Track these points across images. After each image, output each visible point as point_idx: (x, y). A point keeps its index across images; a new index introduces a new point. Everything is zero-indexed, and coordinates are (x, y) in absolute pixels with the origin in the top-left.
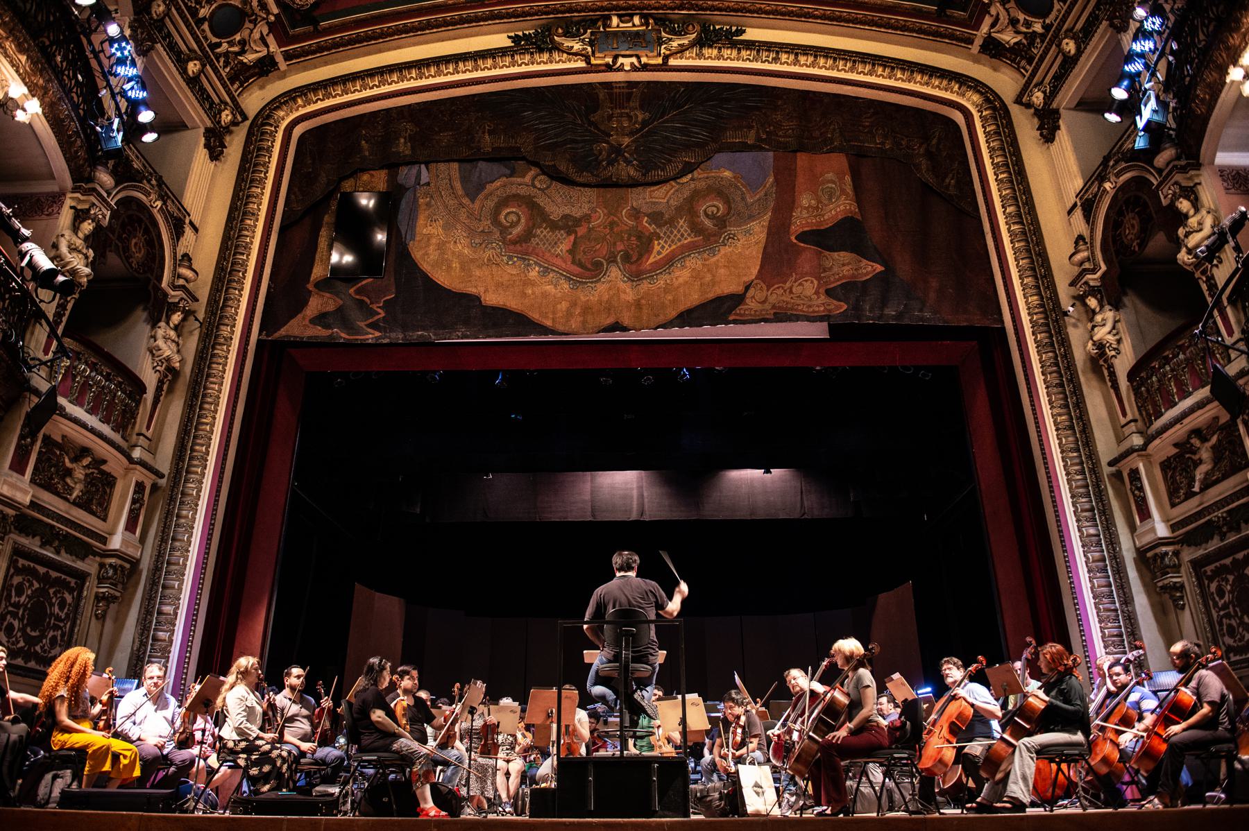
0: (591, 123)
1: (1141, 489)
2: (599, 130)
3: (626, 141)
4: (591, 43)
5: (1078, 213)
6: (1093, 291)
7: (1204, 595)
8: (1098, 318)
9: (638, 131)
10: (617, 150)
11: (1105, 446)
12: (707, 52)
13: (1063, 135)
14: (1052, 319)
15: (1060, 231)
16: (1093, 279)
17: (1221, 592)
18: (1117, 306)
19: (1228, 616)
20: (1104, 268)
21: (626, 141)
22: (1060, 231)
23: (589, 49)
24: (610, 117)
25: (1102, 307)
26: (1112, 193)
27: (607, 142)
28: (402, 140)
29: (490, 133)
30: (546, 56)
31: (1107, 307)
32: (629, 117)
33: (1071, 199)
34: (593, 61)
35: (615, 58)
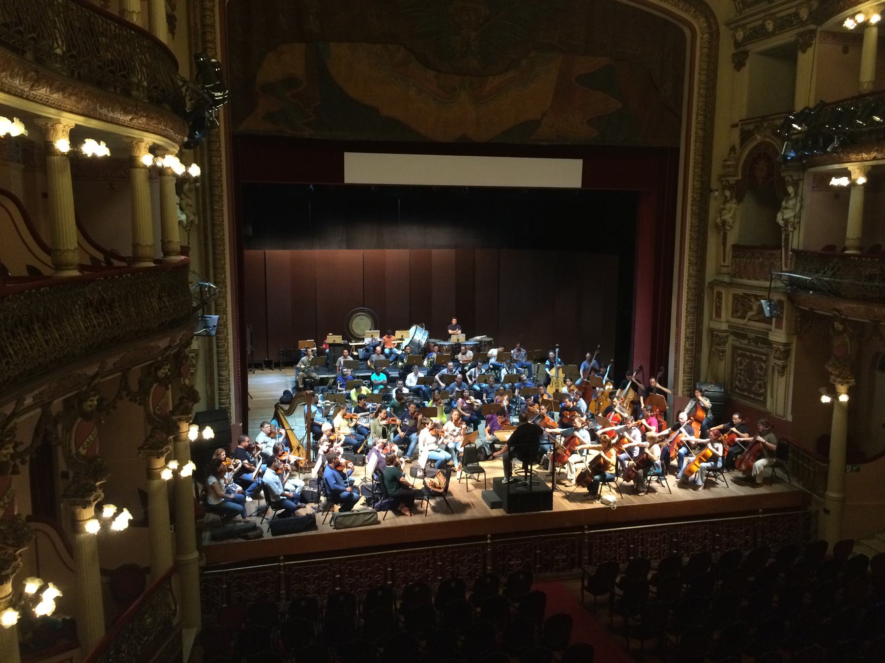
1: (721, 303)
5: (736, 132)
6: (731, 188)
7: (733, 362)
8: (728, 205)
11: (710, 275)
13: (746, 70)
15: (725, 139)
16: (732, 180)
17: (741, 364)
18: (740, 200)
19: (740, 374)
20: (740, 177)
22: (725, 139)
25: (732, 198)
26: (759, 141)
31: (734, 201)
33: (736, 120)
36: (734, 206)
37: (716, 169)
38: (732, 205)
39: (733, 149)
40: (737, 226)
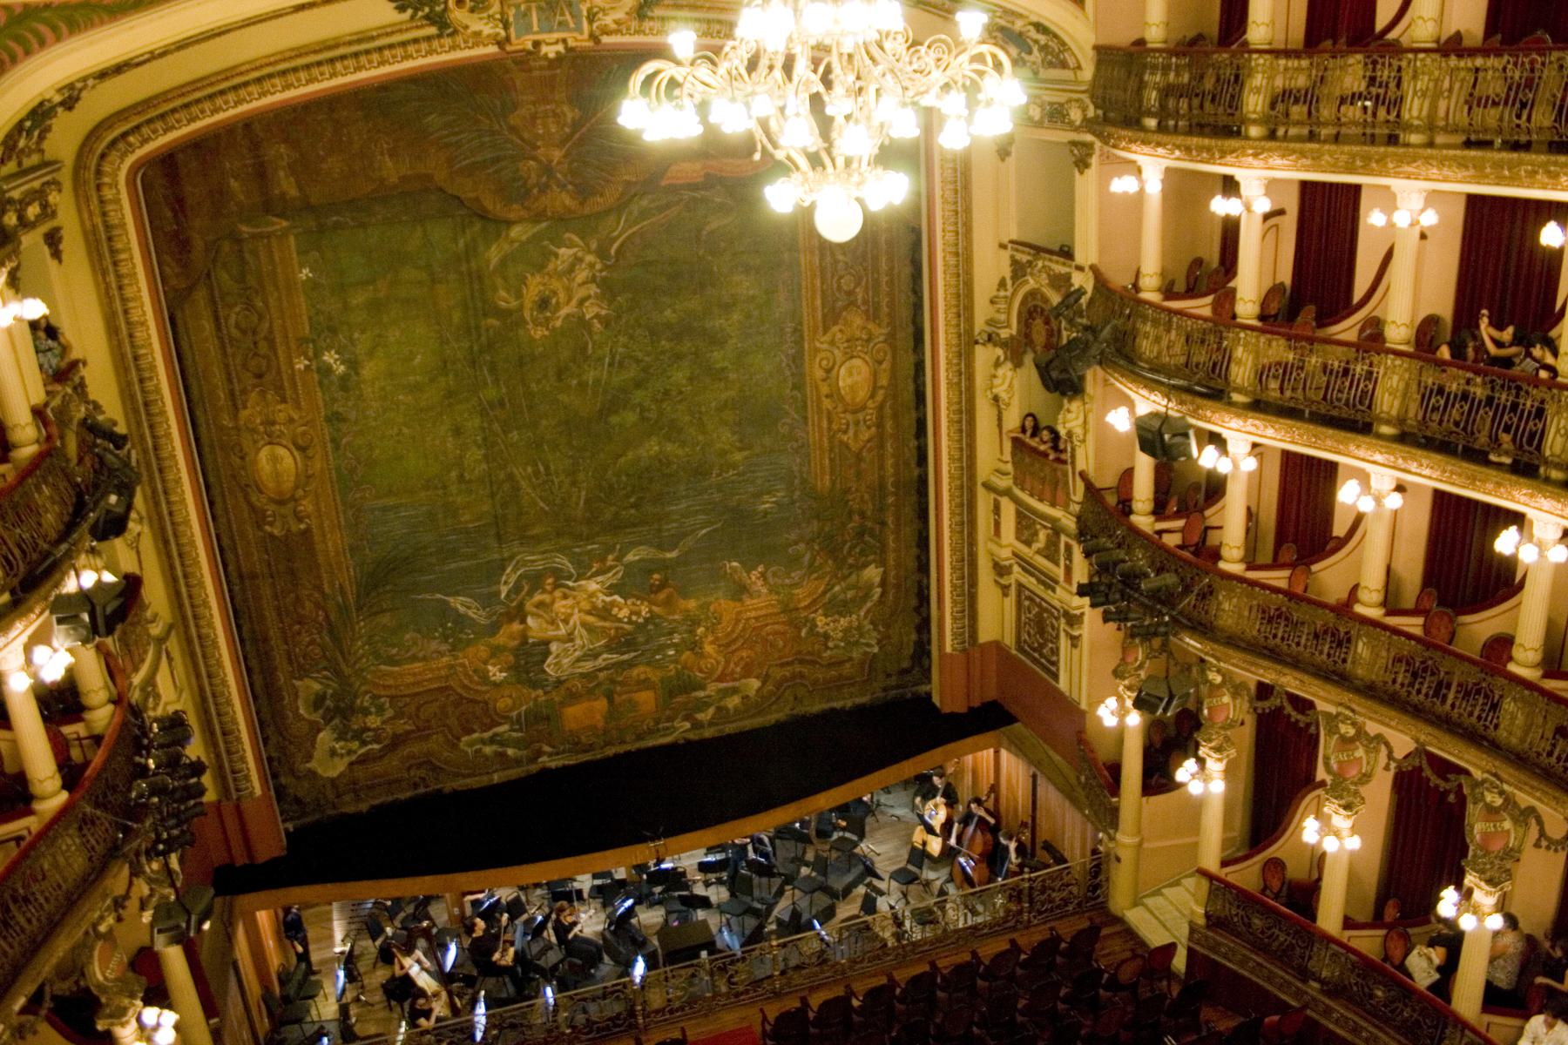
0: (513, 129)
2: (523, 140)
3: (557, 154)
4: (506, 26)
8: (1000, 372)
9: (569, 137)
10: (547, 169)
12: (647, 24)
14: (966, 345)
18: (1018, 364)
20: (1014, 332)
21: (557, 154)
23: (503, 33)
24: (534, 117)
27: (534, 158)
28: (282, 174)
29: (393, 154)
30: (447, 41)
31: (1009, 365)
32: (555, 115)
34: (509, 48)
35: (537, 44)
36: (1010, 374)
37: (982, 312)
38: (1006, 370)
39: (1002, 284)
40: (1015, 402)
